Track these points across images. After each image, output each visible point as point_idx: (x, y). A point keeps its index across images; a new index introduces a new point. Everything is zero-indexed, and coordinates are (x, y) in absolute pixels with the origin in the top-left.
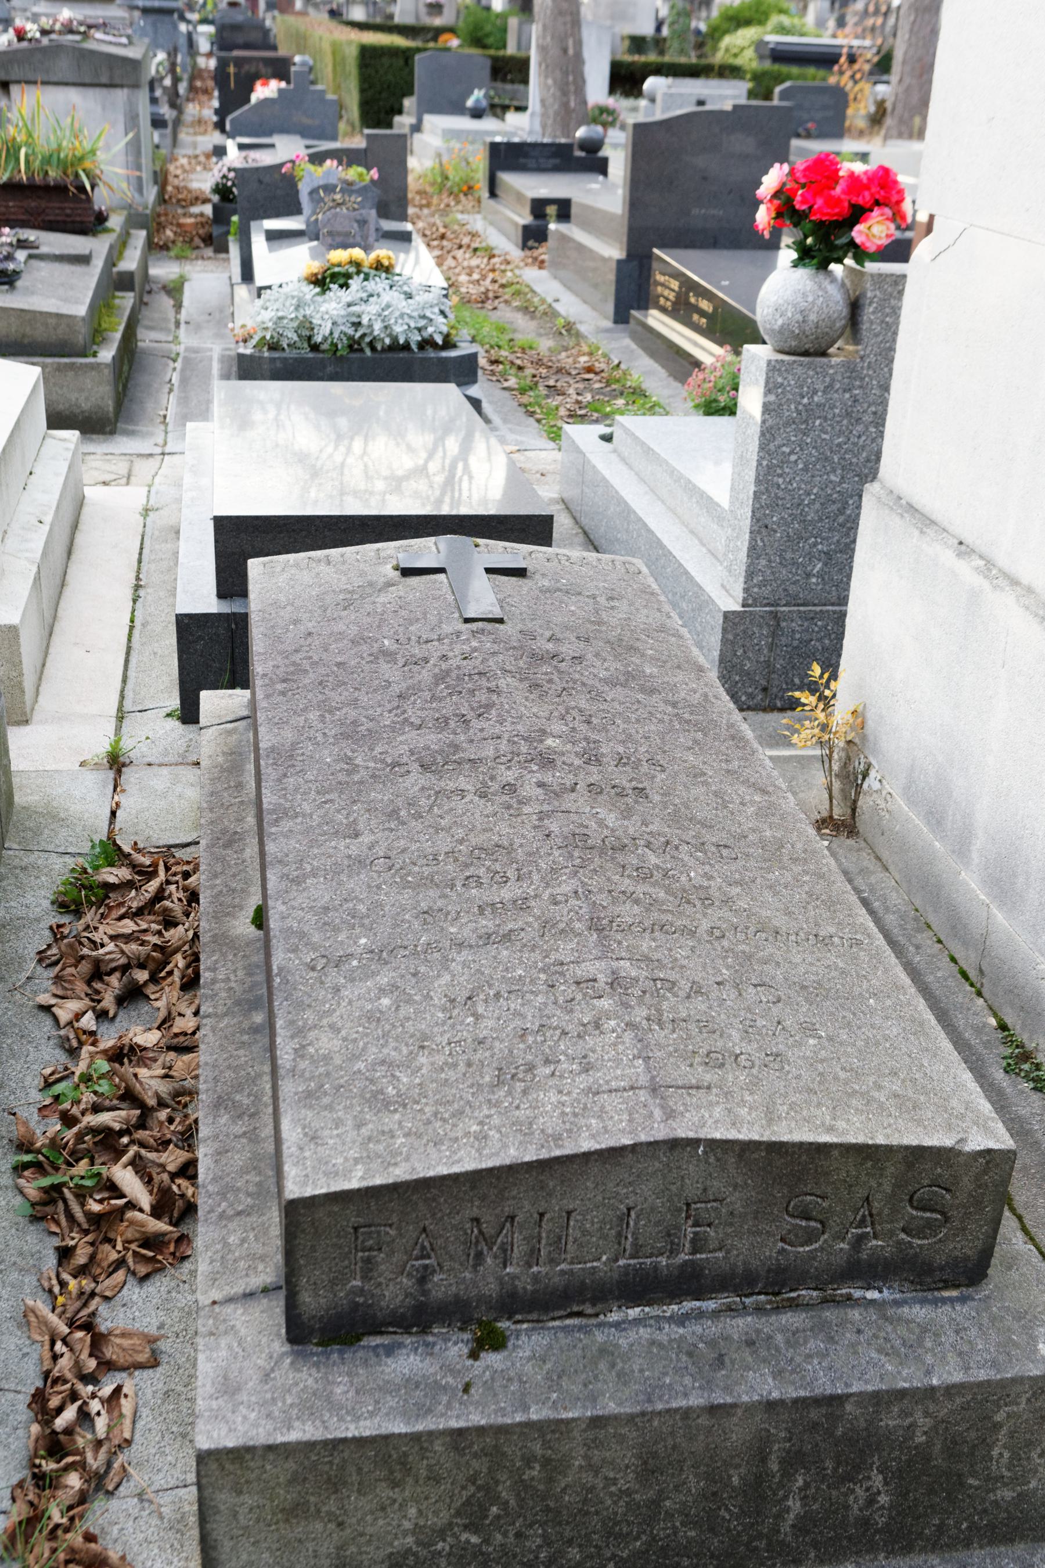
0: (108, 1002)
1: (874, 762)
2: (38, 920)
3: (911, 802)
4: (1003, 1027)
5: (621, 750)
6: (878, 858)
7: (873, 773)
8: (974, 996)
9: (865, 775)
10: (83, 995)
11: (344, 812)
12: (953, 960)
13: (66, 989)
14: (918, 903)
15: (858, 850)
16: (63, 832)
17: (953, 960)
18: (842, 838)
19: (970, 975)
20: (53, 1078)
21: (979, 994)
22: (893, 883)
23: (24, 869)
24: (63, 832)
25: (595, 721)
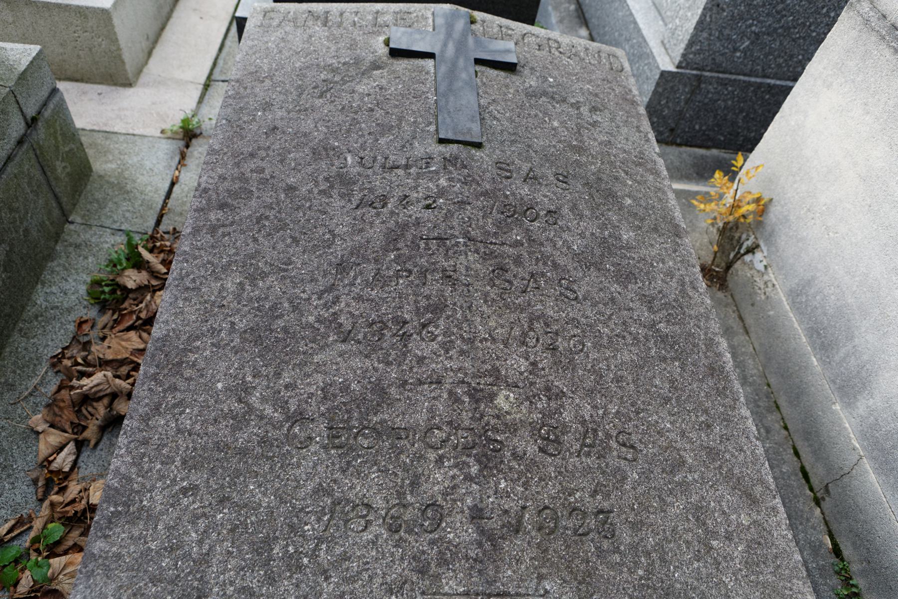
0: (90, 433)
1: (762, 244)
2: (69, 310)
3: (794, 304)
4: (837, 551)
5: (587, 411)
6: (741, 318)
7: (759, 256)
8: (813, 504)
9: (751, 250)
10: (67, 427)
11: (202, 524)
12: (797, 453)
13: (55, 414)
14: (772, 381)
15: (726, 306)
16: (125, 206)
17: (797, 453)
18: (714, 288)
19: (812, 480)
20: (9, 536)
21: (818, 502)
22: (751, 349)
23: (78, 246)
24: (125, 206)
25: (561, 343)
